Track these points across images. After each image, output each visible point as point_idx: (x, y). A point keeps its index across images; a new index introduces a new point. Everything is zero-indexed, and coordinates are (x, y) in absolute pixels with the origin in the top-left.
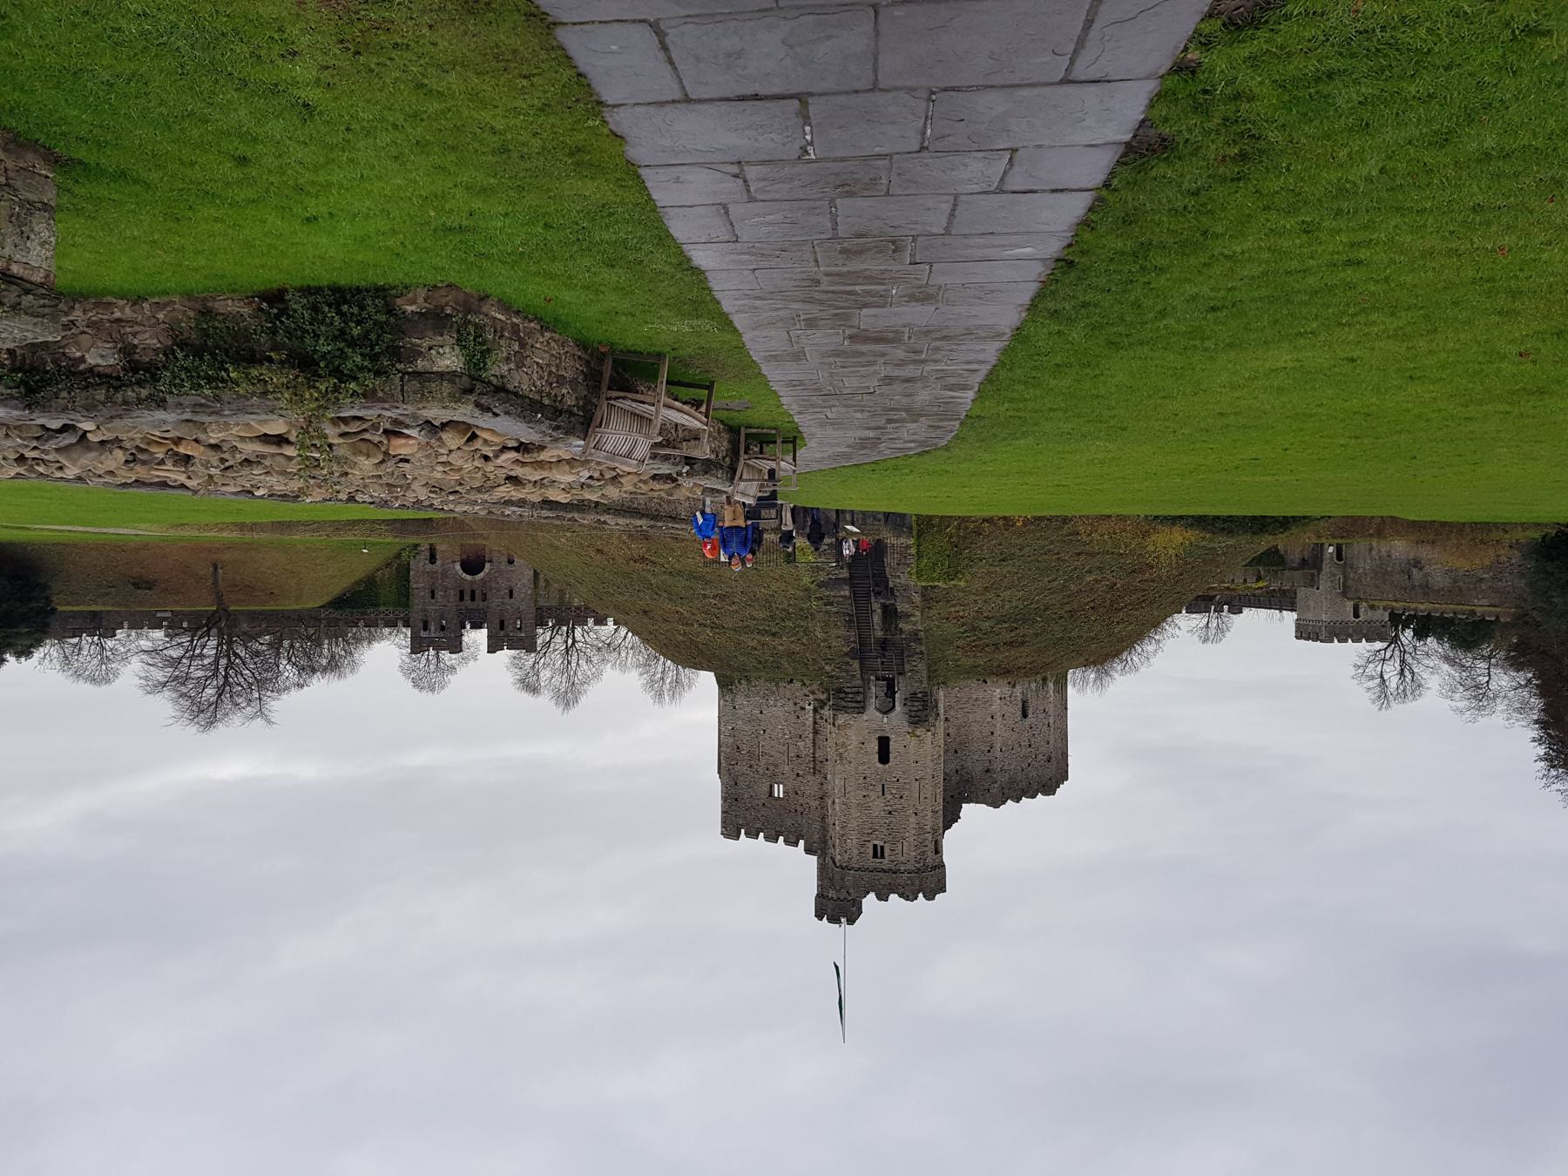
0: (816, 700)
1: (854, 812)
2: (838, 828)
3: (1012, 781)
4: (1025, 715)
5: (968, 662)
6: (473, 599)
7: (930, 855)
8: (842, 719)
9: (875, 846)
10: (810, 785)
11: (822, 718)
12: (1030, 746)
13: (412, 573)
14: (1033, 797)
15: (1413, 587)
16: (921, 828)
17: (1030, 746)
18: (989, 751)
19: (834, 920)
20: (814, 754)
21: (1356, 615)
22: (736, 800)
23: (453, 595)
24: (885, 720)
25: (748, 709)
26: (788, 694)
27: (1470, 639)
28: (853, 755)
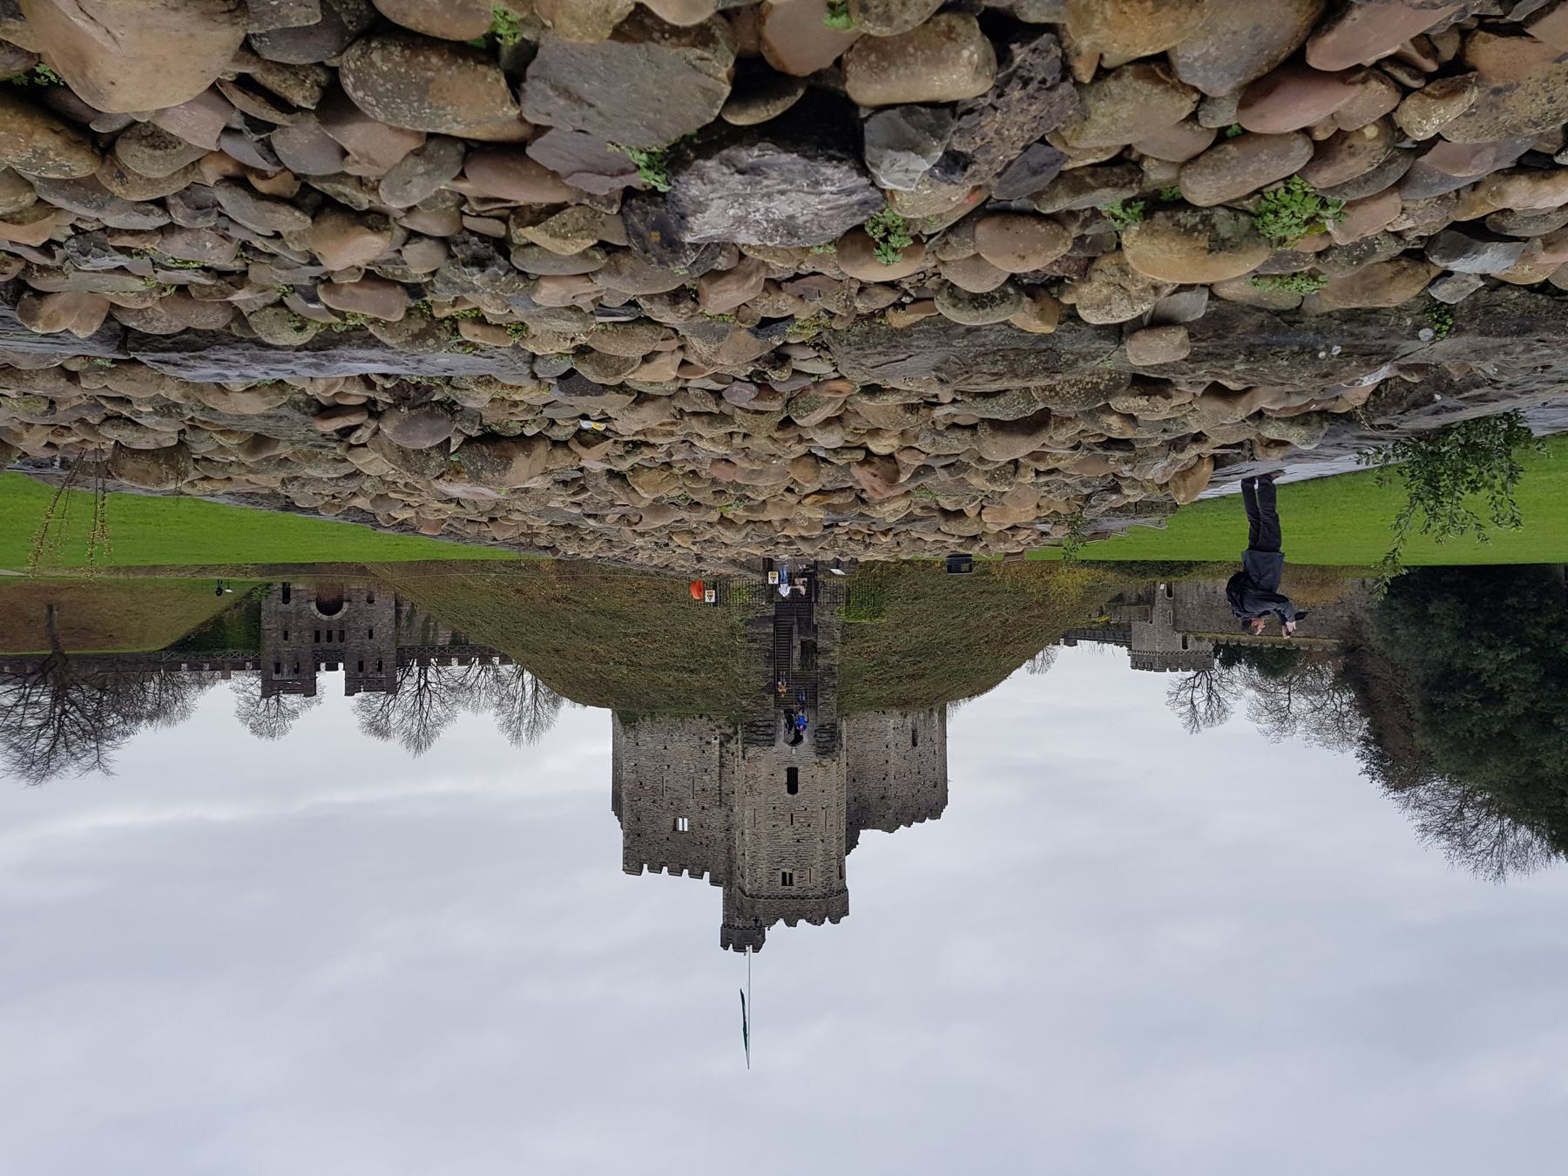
0: (722, 734)
2: (747, 858)
3: (904, 807)
4: (915, 744)
5: (872, 695)
6: (329, 639)
7: (835, 879)
8: (752, 751)
9: (784, 874)
10: (716, 818)
11: (728, 752)
14: (922, 821)
16: (827, 853)
18: (884, 779)
19: (740, 948)
21: (1185, 647)
23: (308, 636)
24: (794, 751)
25: (651, 746)
26: (694, 729)
27: (1276, 667)
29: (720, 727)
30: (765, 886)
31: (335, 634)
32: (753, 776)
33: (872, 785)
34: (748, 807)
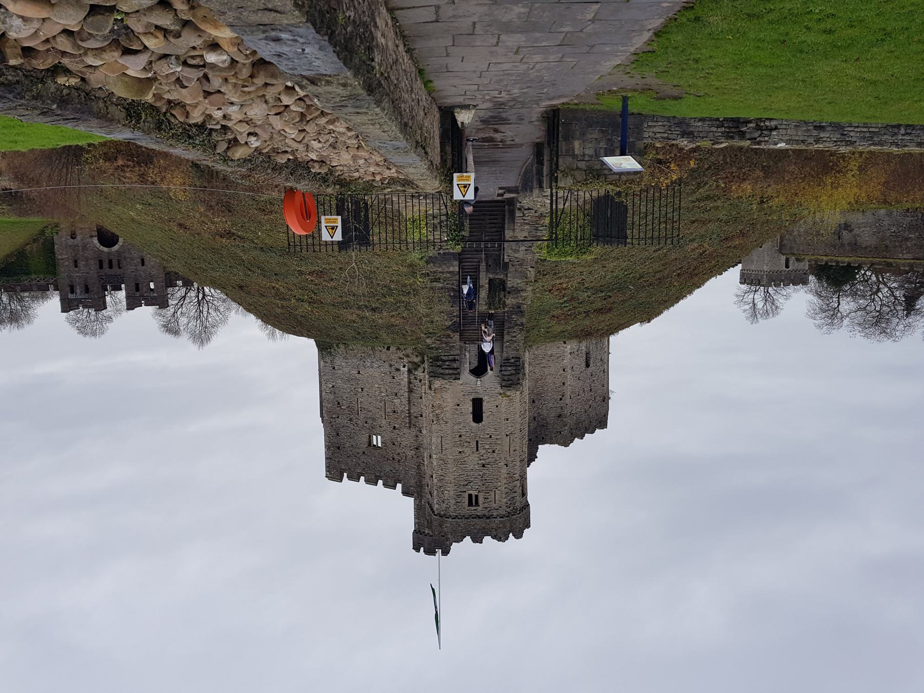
0: (410, 362)
1: (451, 467)
2: (435, 481)
3: (578, 422)
4: (588, 365)
5: (559, 328)
6: (111, 266)
8: (437, 383)
9: (470, 496)
10: (406, 437)
11: (416, 378)
12: (591, 390)
13: (56, 247)
14: (592, 432)
15: (843, 245)
16: (511, 476)
17: (591, 390)
18: (561, 399)
19: (430, 552)
20: (409, 410)
21: (787, 266)
22: (339, 448)
23: (94, 264)
24: (479, 383)
25: (347, 370)
26: (384, 357)
28: (448, 415)
29: (408, 356)
30: (452, 509)
31: (115, 262)
32: (440, 406)
33: (550, 405)
34: (435, 434)
